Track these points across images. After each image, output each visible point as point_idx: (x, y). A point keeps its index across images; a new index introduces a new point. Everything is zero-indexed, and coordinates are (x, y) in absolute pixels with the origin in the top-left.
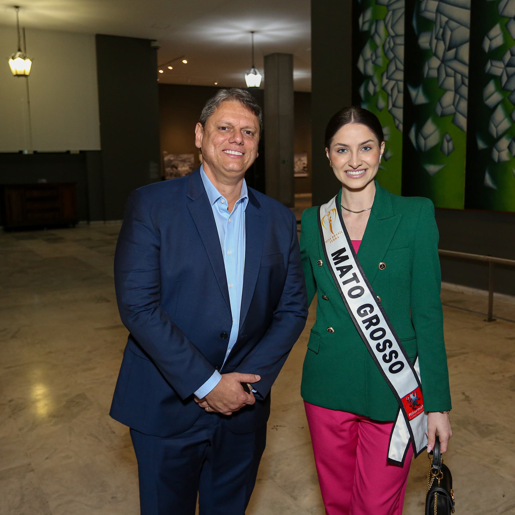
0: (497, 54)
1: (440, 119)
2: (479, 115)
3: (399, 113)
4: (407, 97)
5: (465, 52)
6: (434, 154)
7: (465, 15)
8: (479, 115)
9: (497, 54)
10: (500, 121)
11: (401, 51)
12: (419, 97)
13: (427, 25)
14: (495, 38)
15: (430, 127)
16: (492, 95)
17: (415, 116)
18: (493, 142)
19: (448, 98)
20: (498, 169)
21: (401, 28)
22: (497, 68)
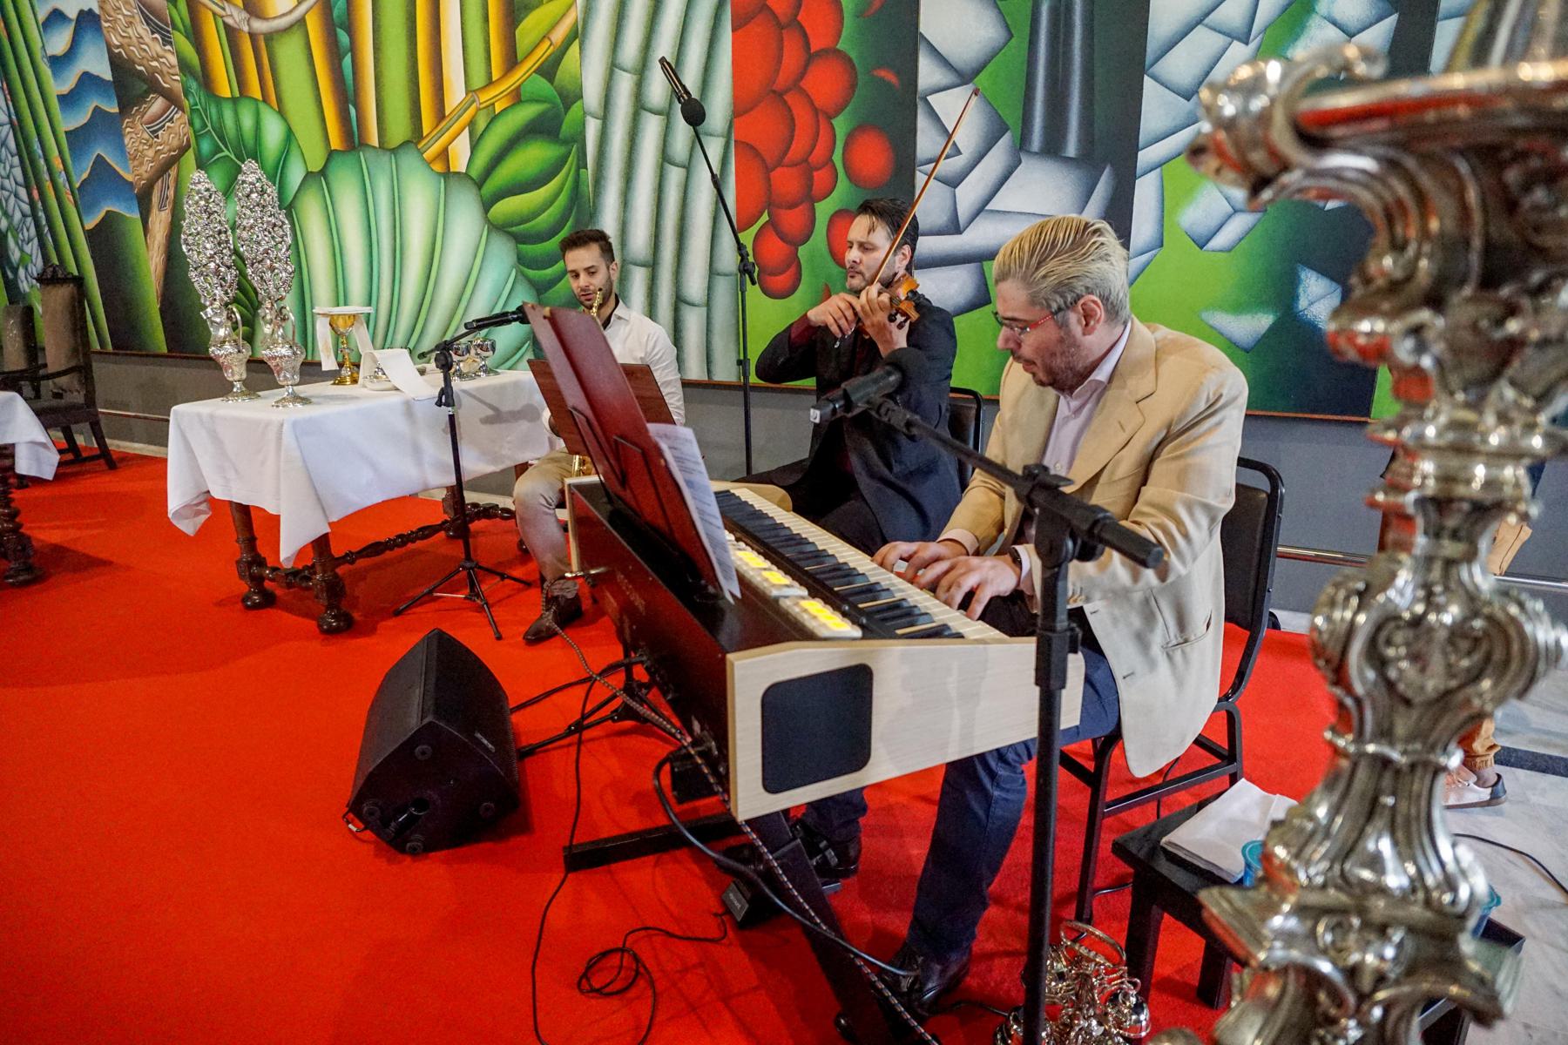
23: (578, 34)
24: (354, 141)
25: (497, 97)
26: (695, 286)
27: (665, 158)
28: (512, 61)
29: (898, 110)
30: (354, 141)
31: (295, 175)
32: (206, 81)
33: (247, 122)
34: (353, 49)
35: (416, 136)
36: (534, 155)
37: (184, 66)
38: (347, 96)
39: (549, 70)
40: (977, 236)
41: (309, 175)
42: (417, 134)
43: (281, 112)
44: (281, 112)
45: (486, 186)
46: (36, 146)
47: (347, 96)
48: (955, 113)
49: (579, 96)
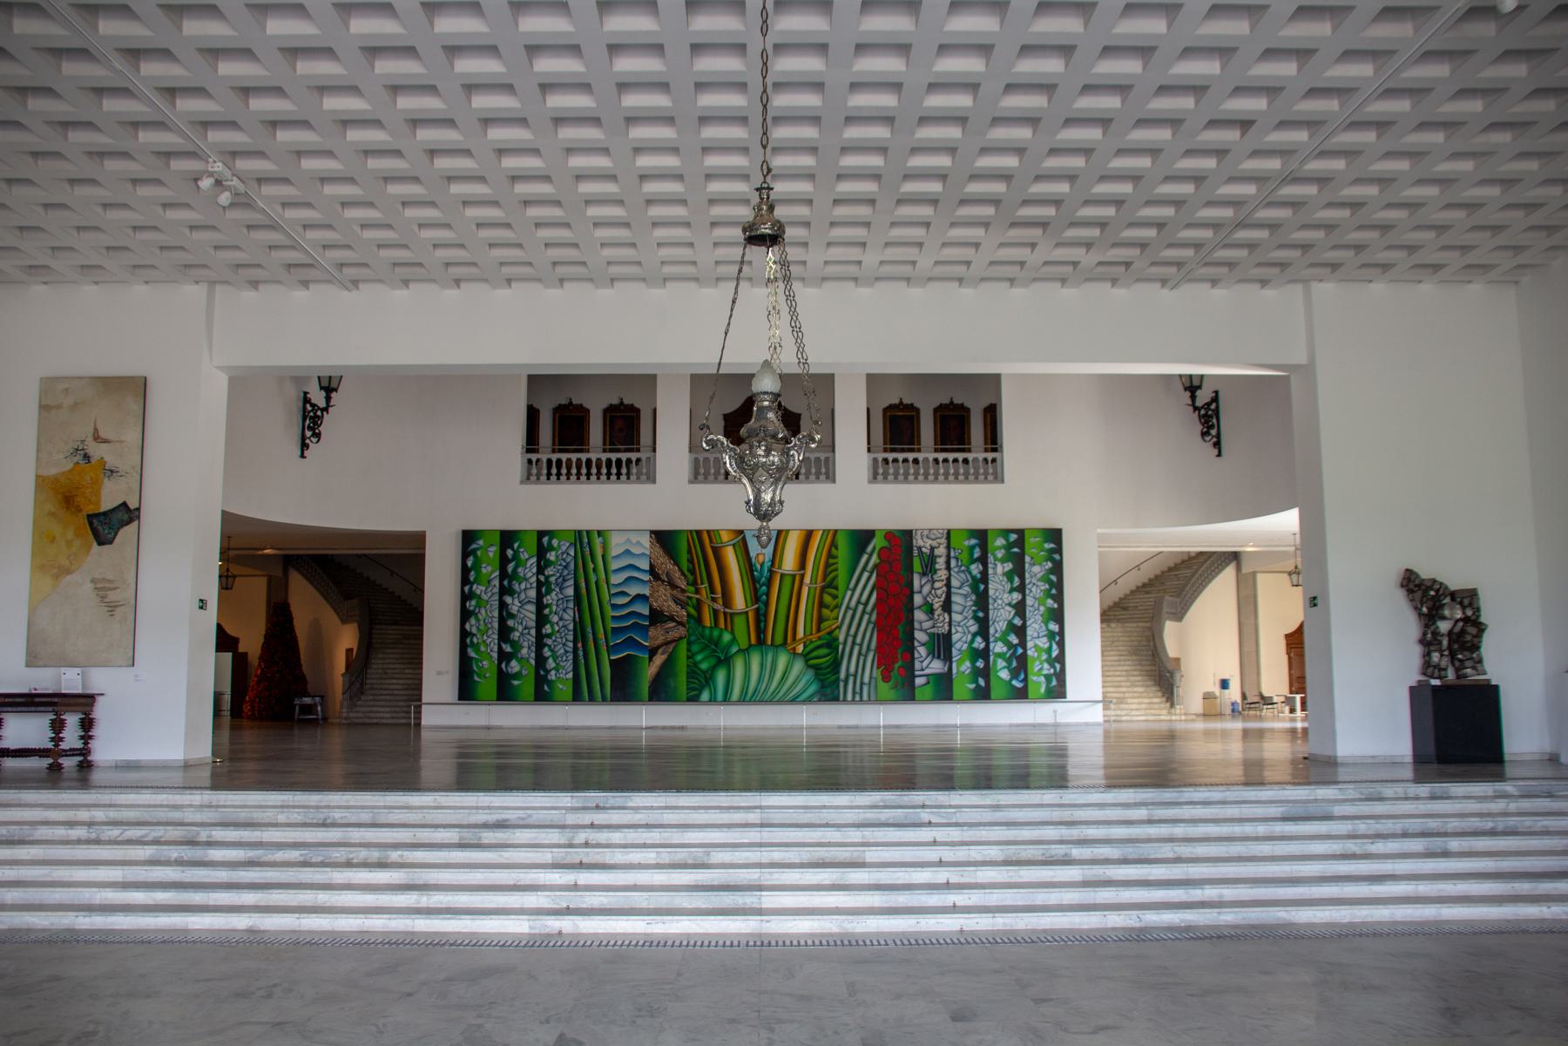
0: (549, 636)
1: (520, 660)
2: (541, 661)
3: (495, 655)
4: (500, 649)
5: (533, 632)
6: (517, 676)
7: (533, 617)
8: (541, 661)
9: (549, 636)
10: (551, 664)
11: (496, 625)
12: (507, 648)
13: (512, 616)
14: (547, 629)
15: (514, 663)
16: (547, 652)
17: (504, 657)
18: (548, 672)
19: (524, 651)
20: (550, 683)
21: (496, 614)
22: (549, 642)
23: (839, 627)
24: (761, 642)
25: (814, 638)
26: (866, 680)
27: (860, 654)
28: (819, 630)
29: (912, 648)
30: (761, 642)
31: (734, 649)
32: (699, 620)
33: (716, 633)
34: (766, 621)
35: (785, 643)
36: (824, 651)
37: (689, 615)
38: (761, 632)
39: (830, 633)
40: (927, 671)
41: (740, 651)
42: (785, 643)
43: (732, 632)
44: (732, 632)
45: (806, 656)
46: (589, 629)
47: (761, 632)
48: (922, 651)
49: (836, 639)
